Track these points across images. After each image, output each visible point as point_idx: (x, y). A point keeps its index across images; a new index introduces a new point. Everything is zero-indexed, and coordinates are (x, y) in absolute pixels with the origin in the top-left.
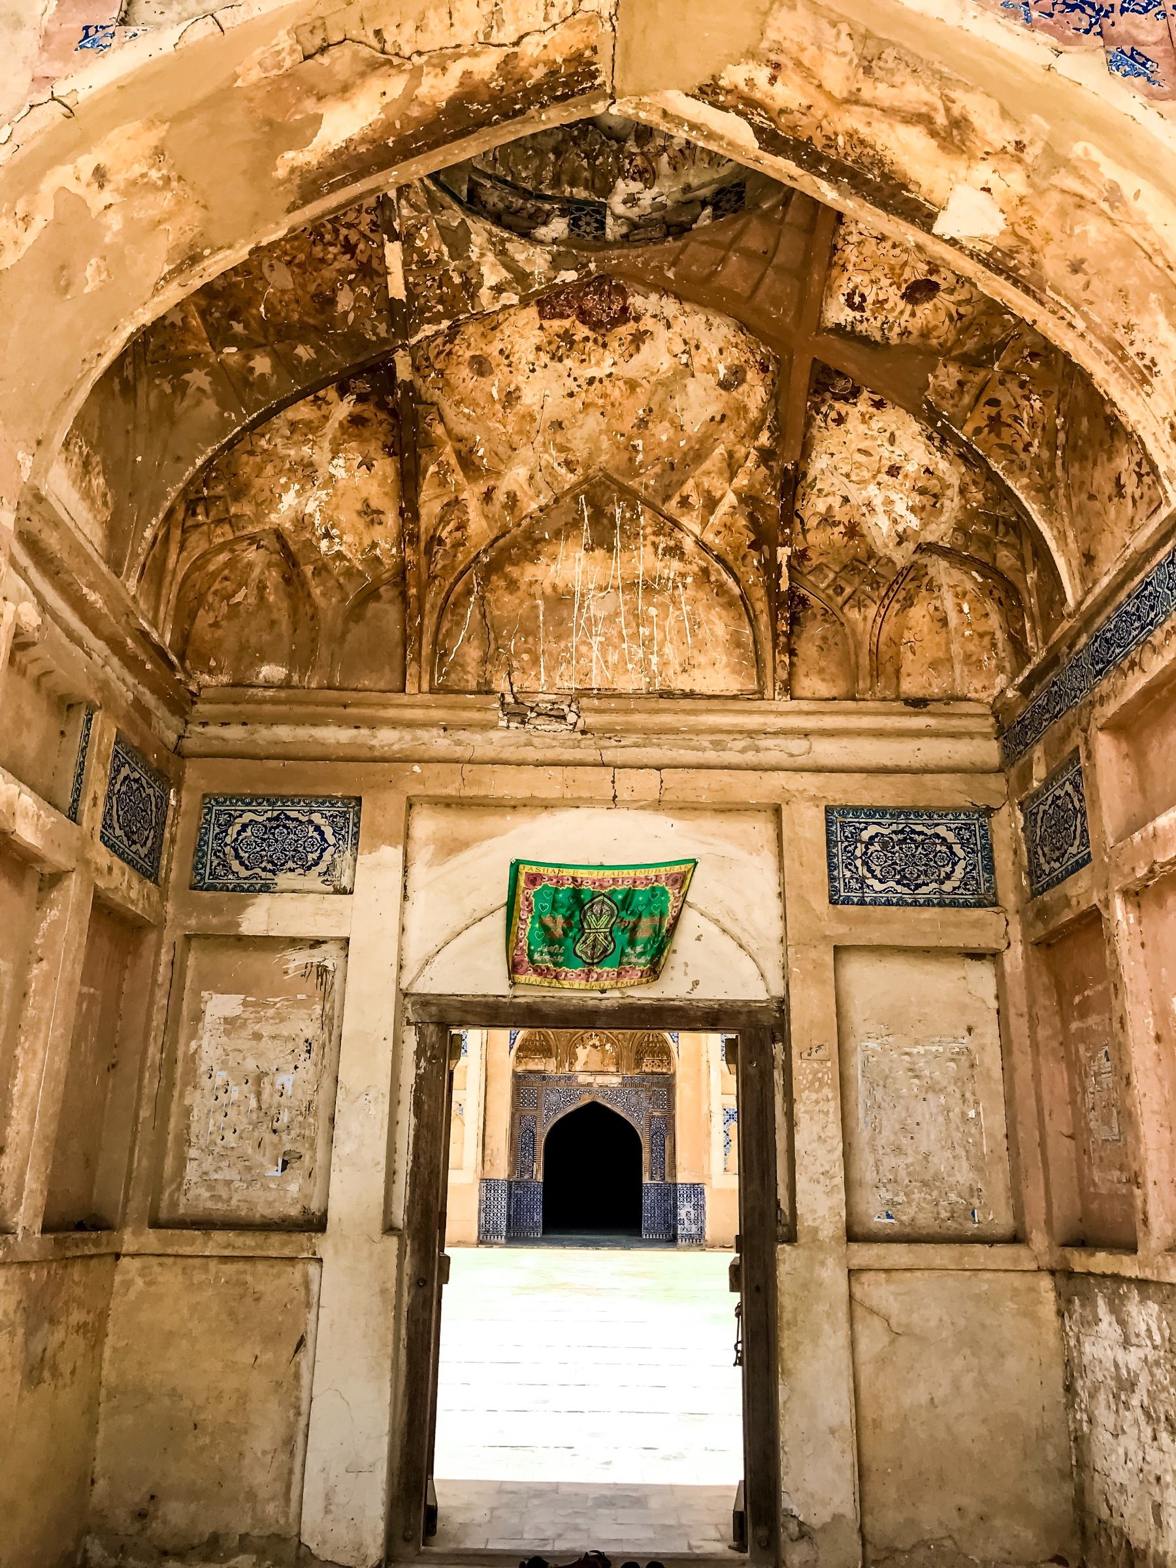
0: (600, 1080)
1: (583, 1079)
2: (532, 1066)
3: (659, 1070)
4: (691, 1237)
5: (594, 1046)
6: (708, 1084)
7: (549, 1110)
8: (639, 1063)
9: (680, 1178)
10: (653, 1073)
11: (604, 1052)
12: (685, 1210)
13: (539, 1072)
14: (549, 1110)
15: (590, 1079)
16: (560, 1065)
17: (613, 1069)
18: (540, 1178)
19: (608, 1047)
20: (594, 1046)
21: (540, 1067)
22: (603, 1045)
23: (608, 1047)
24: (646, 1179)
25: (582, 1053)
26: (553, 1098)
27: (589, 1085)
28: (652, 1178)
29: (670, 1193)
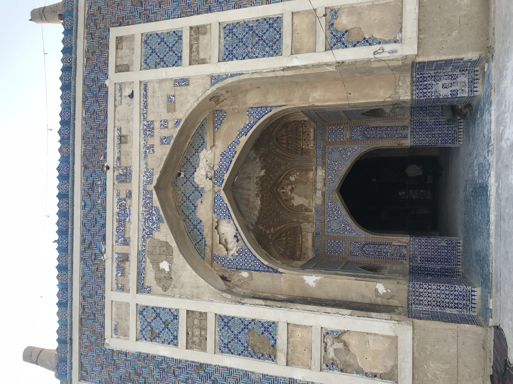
0: (319, 185)
1: (319, 202)
2: (309, 244)
3: (312, 135)
4: (472, 82)
5: (292, 190)
6: (306, 67)
7: (345, 230)
8: (304, 152)
9: (405, 94)
10: (314, 140)
11: (296, 182)
12: (442, 90)
13: (313, 238)
14: (345, 230)
15: (319, 193)
16: (307, 219)
17: (311, 174)
18: (405, 239)
19: (292, 179)
20: (292, 190)
21: (310, 237)
22: (291, 183)
23: (292, 179)
24: (408, 143)
25: (298, 201)
26: (335, 226)
27: (323, 194)
28: (406, 137)
29: (422, 109)
